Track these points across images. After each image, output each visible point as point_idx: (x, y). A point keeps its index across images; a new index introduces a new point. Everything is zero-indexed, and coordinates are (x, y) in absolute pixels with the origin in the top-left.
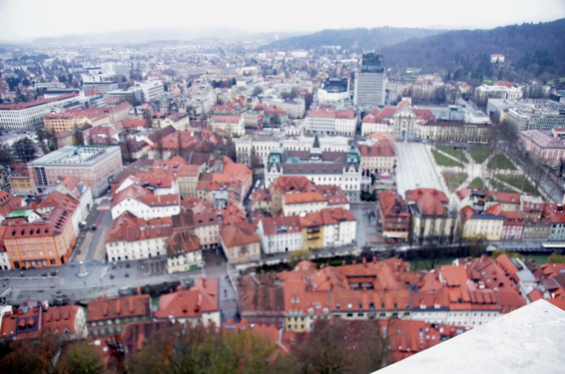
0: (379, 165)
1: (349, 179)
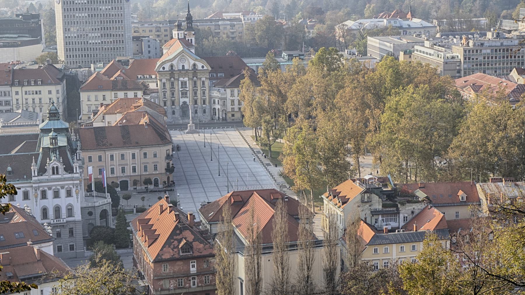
0: (129, 172)
1: (50, 194)
